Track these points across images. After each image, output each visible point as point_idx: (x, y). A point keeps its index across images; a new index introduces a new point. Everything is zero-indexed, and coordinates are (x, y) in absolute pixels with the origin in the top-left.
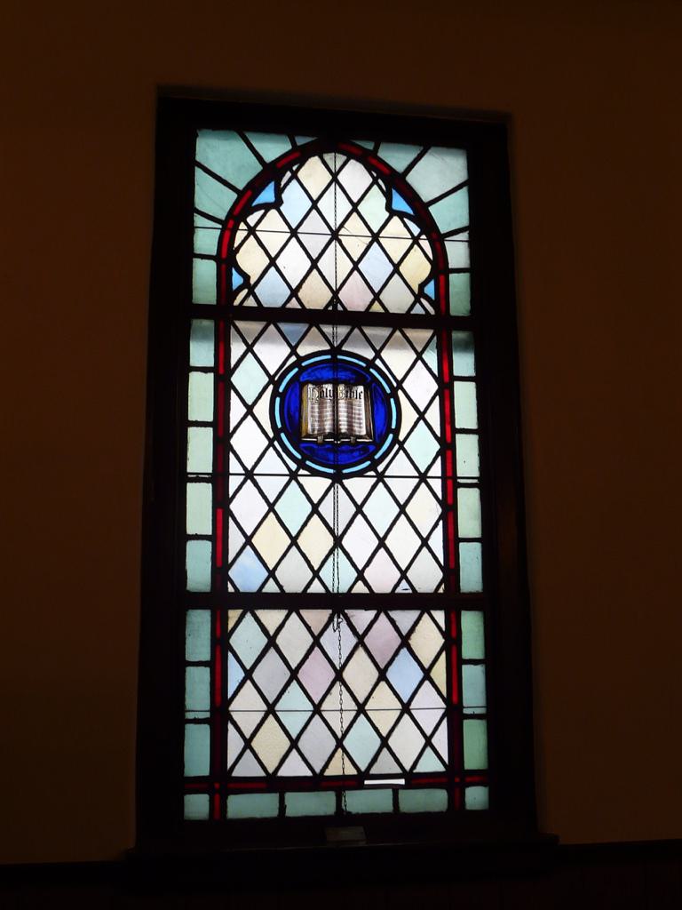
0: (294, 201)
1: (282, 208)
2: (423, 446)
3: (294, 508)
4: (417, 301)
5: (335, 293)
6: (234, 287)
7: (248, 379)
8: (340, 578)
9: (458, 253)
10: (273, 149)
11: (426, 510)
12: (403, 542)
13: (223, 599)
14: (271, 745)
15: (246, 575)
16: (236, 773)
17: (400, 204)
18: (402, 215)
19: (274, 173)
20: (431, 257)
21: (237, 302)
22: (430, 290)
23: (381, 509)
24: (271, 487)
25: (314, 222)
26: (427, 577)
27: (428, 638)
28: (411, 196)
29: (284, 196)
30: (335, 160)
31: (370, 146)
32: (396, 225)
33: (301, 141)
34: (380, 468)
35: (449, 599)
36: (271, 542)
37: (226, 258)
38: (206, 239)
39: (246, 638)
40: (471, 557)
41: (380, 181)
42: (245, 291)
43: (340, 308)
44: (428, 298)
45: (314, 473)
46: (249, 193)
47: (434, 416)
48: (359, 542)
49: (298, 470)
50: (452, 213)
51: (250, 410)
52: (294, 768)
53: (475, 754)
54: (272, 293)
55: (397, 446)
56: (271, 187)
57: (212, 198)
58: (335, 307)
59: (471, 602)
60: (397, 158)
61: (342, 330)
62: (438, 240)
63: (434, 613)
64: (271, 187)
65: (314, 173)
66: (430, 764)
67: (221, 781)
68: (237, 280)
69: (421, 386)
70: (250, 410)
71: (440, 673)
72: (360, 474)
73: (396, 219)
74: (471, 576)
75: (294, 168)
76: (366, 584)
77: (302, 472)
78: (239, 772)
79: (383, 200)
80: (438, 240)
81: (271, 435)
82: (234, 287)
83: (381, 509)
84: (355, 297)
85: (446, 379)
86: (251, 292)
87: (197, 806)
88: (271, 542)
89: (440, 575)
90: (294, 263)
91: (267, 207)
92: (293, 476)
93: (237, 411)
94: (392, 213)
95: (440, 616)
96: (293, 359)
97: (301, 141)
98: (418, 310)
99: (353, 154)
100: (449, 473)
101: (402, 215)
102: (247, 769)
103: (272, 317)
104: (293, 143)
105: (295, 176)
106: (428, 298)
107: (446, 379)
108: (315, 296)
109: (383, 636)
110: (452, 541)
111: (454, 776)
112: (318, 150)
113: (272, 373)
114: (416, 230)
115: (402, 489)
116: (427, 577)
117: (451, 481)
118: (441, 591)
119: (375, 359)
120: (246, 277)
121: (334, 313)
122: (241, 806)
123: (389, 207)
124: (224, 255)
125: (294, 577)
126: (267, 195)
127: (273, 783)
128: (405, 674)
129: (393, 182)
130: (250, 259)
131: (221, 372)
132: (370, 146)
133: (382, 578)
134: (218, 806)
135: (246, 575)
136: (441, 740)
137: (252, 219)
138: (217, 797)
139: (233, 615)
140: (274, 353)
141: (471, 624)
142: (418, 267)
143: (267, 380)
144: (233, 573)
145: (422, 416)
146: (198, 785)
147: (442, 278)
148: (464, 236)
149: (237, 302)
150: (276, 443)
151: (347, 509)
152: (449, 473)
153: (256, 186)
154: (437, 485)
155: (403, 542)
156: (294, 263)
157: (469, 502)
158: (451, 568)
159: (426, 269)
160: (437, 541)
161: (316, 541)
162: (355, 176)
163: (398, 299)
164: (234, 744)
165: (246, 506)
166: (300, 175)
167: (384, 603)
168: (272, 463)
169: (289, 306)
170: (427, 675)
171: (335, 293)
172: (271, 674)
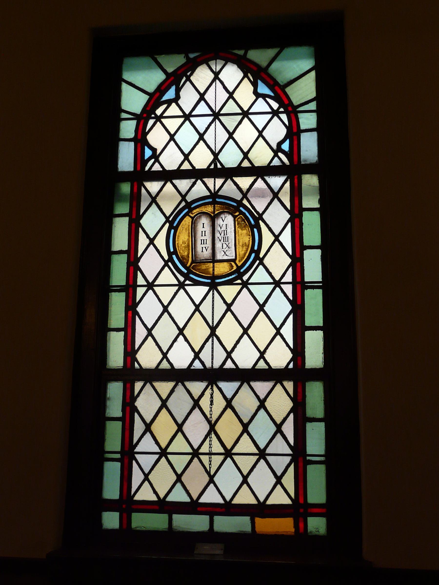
0: (188, 97)
1: (179, 102)
2: (278, 261)
3: (181, 308)
4: (276, 155)
5: (216, 155)
6: (146, 157)
7: (152, 221)
8: (213, 357)
9: (308, 120)
10: (173, 63)
11: (279, 307)
12: (262, 331)
13: (132, 374)
14: (163, 479)
15: (148, 357)
16: (137, 498)
17: (263, 89)
18: (264, 96)
19: (176, 79)
20: (287, 123)
21: (147, 168)
22: (286, 146)
23: (245, 307)
24: (166, 294)
25: (202, 109)
26: (280, 357)
27: (280, 401)
28: (272, 83)
29: (182, 93)
30: (217, 65)
31: (241, 52)
32: (261, 105)
33: (192, 56)
34: (245, 278)
35: (296, 374)
36: (165, 332)
37: (140, 140)
38: (128, 128)
39: (147, 402)
40: (314, 342)
41: (249, 75)
42: (153, 160)
43: (219, 166)
44: (284, 152)
45: (196, 283)
46: (157, 95)
47: (286, 238)
48: (229, 331)
49: (185, 281)
50: (304, 90)
51: (152, 241)
52: (178, 496)
53: (317, 493)
54: (171, 160)
55: (258, 262)
56: (173, 88)
57: (133, 101)
58: (216, 165)
59: (314, 374)
60: (259, 56)
61: (219, 182)
62: (292, 111)
63: (285, 383)
64: (173, 88)
65: (202, 76)
66: (280, 498)
67: (127, 504)
68: (148, 153)
69: (277, 216)
70: (152, 241)
71: (289, 429)
72: (230, 283)
73: (260, 100)
74: (314, 356)
75: (189, 74)
76: (168, 361)
77: (187, 282)
78: (138, 497)
79: (252, 88)
80: (292, 111)
81: (166, 258)
82: (146, 157)
83: (245, 307)
84: (230, 158)
85: (297, 211)
86: (157, 160)
87: (111, 520)
88: (165, 332)
89: (290, 355)
90: (186, 137)
91: (169, 103)
92: (181, 286)
93: (143, 242)
94: (258, 95)
95: (289, 385)
96: (183, 204)
97: (192, 56)
98: (276, 162)
99: (229, 59)
100: (299, 279)
101: (264, 96)
102: (145, 494)
103: (167, 176)
104: (187, 57)
105: (188, 79)
106: (284, 152)
107: (297, 211)
108: (201, 159)
109: (246, 401)
110: (300, 329)
111: (299, 508)
112: (204, 60)
113: (168, 215)
114: (275, 105)
115: (261, 292)
116: (280, 357)
117: (300, 285)
118: (291, 366)
119: (242, 199)
120: (154, 150)
121: (217, 171)
122: (141, 521)
123: (255, 92)
124: (139, 137)
125: (181, 358)
126: (170, 94)
127: (162, 506)
128: (262, 429)
129: (256, 73)
130: (157, 137)
131: (134, 216)
132: (241, 52)
133: (245, 357)
134: (125, 520)
135: (148, 357)
136: (289, 481)
137: (159, 112)
138: (125, 515)
139: (138, 385)
140: (169, 201)
141: (315, 393)
142: (277, 131)
143: (164, 220)
144: (139, 356)
145: (277, 238)
146: (111, 505)
147: (295, 138)
148: (313, 106)
149: (147, 168)
150: (170, 264)
151: (221, 308)
152: (299, 279)
153: (162, 89)
154: (289, 289)
155: (262, 331)
156: (186, 137)
157: (314, 301)
158: (298, 350)
159: (283, 132)
160: (288, 331)
161: (198, 332)
162: (231, 74)
163: (262, 156)
164: (137, 477)
165: (148, 309)
166: (192, 78)
167: (245, 376)
168: (167, 277)
169: (182, 168)
170: (279, 428)
171: (216, 155)
172: (164, 428)
